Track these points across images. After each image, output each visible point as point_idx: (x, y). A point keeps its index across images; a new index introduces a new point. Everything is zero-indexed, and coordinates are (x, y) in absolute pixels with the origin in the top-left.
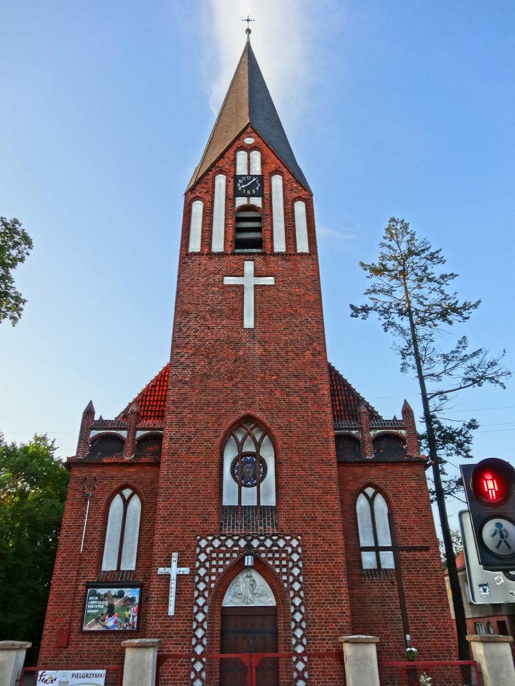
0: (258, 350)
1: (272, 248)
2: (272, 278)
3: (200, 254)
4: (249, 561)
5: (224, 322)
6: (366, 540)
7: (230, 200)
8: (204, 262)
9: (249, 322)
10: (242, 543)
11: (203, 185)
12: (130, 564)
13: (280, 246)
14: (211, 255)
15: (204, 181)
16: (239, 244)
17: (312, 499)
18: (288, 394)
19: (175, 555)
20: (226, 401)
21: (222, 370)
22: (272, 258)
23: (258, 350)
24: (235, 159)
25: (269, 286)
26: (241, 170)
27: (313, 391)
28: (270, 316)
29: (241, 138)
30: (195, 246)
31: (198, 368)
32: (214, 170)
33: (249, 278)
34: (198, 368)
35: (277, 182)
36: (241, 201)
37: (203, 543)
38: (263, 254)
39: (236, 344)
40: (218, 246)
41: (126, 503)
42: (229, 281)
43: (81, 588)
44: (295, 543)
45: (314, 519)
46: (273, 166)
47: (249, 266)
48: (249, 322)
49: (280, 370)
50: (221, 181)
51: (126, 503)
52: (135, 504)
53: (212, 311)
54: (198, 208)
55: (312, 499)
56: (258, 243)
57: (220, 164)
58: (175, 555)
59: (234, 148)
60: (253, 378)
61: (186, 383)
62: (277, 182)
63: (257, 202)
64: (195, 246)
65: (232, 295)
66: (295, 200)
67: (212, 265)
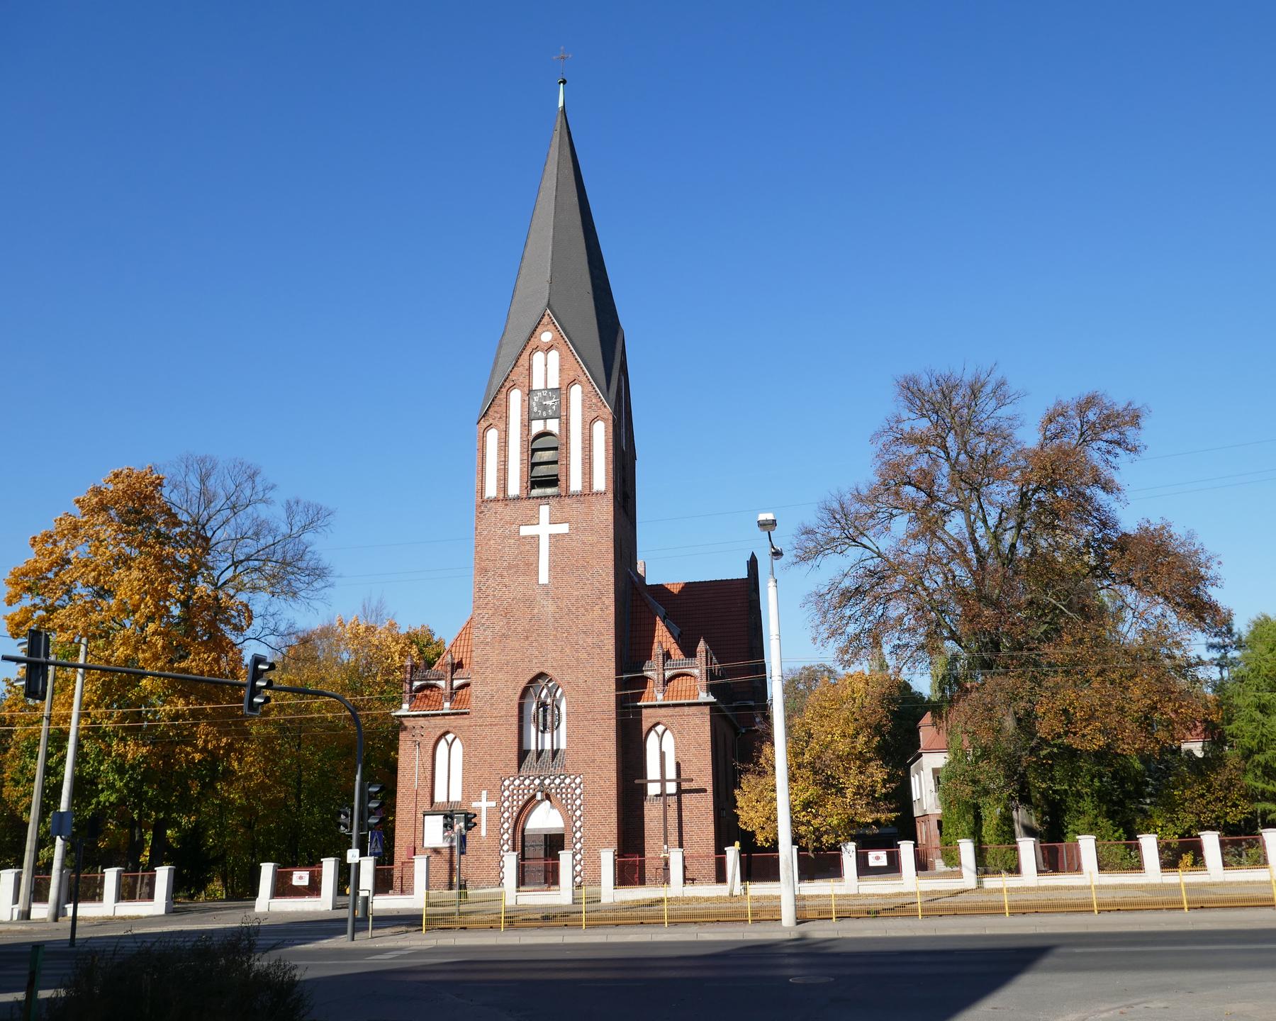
0: (550, 607)
1: (568, 487)
2: (567, 525)
3: (496, 500)
4: (539, 796)
5: (521, 579)
6: (653, 771)
7: (527, 426)
8: (500, 510)
9: (544, 577)
10: (537, 782)
11: (496, 409)
12: (456, 796)
13: (576, 484)
14: (505, 499)
15: (497, 401)
16: (537, 483)
17: (593, 745)
18: (577, 651)
19: (484, 792)
20: (523, 660)
21: (519, 630)
22: (567, 501)
23: (550, 607)
24: (530, 368)
25: (563, 535)
26: (538, 384)
27: (599, 647)
28: (563, 569)
29: (537, 333)
30: (491, 491)
31: (497, 628)
32: (508, 385)
33: (544, 527)
34: (497, 628)
35: (576, 393)
36: (537, 427)
37: (507, 783)
38: (559, 496)
39: (529, 602)
40: (514, 488)
41: (450, 745)
42: (525, 531)
43: (420, 816)
44: (578, 781)
45: (593, 761)
46: (572, 373)
47: (544, 510)
48: (544, 577)
49: (570, 627)
50: (516, 397)
51: (450, 745)
52: (457, 745)
53: (509, 567)
54: (492, 436)
55: (593, 745)
56: (552, 481)
57: (512, 377)
58: (484, 792)
59: (528, 350)
60: (547, 636)
61: (487, 644)
62: (576, 393)
63: (553, 426)
64: (491, 491)
65: (528, 547)
66: (593, 421)
67: (508, 512)
